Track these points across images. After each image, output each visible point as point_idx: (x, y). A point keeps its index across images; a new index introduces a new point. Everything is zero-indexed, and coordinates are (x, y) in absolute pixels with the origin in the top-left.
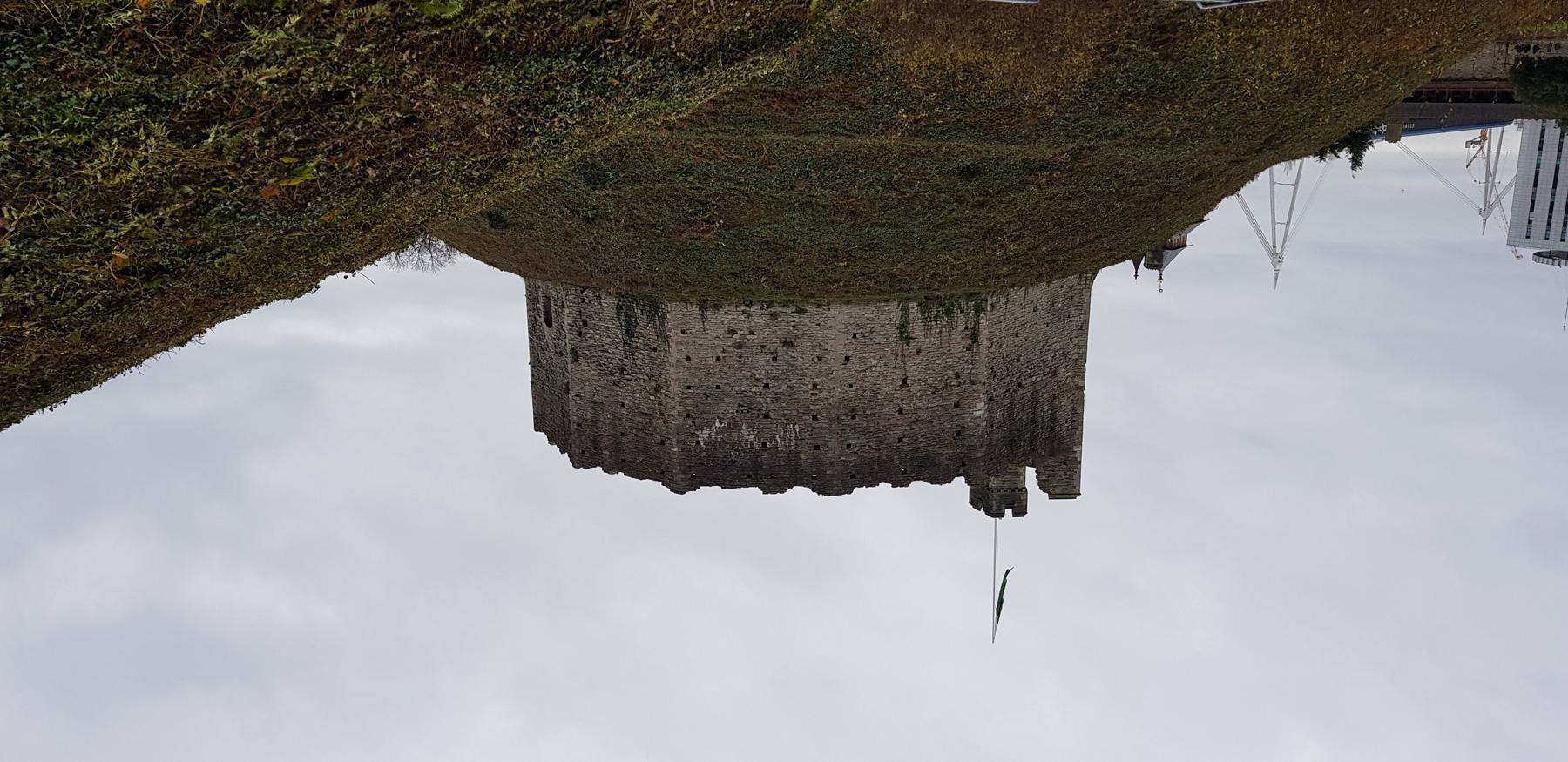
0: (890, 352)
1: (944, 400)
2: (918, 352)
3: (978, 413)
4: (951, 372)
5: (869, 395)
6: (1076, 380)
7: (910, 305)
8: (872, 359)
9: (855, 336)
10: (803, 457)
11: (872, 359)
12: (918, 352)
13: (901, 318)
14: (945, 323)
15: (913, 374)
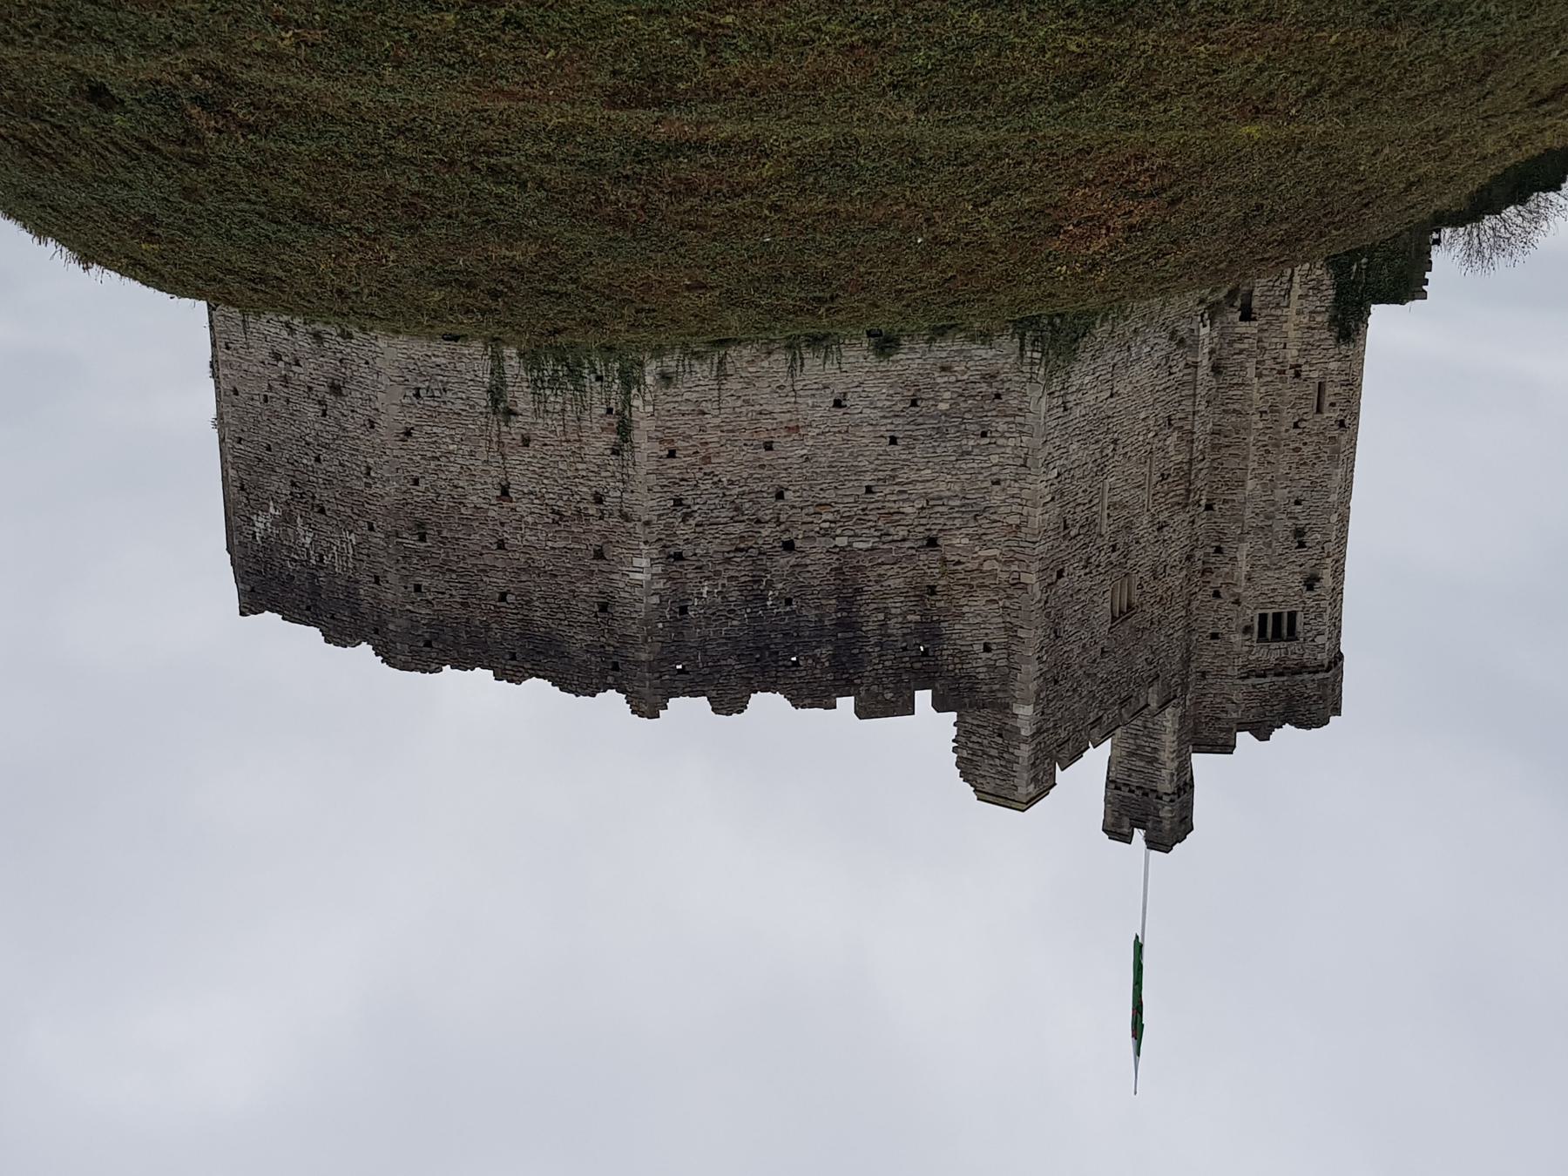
0: (478, 432)
1: (576, 540)
2: (526, 442)
3: (638, 576)
4: (585, 489)
5: (446, 502)
6: (1014, 568)
7: (507, 352)
8: (448, 440)
9: (417, 395)
10: (362, 592)
11: (448, 440)
12: (526, 442)
13: (492, 373)
14: (569, 396)
15: (520, 481)
